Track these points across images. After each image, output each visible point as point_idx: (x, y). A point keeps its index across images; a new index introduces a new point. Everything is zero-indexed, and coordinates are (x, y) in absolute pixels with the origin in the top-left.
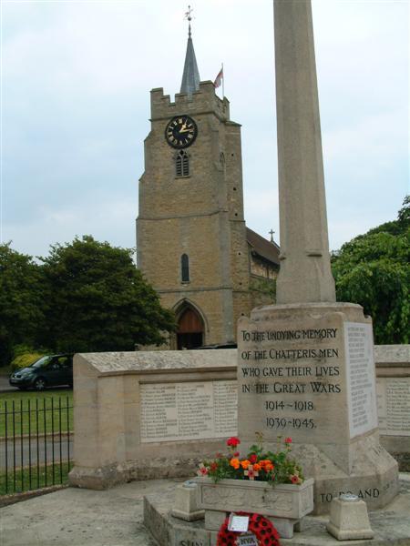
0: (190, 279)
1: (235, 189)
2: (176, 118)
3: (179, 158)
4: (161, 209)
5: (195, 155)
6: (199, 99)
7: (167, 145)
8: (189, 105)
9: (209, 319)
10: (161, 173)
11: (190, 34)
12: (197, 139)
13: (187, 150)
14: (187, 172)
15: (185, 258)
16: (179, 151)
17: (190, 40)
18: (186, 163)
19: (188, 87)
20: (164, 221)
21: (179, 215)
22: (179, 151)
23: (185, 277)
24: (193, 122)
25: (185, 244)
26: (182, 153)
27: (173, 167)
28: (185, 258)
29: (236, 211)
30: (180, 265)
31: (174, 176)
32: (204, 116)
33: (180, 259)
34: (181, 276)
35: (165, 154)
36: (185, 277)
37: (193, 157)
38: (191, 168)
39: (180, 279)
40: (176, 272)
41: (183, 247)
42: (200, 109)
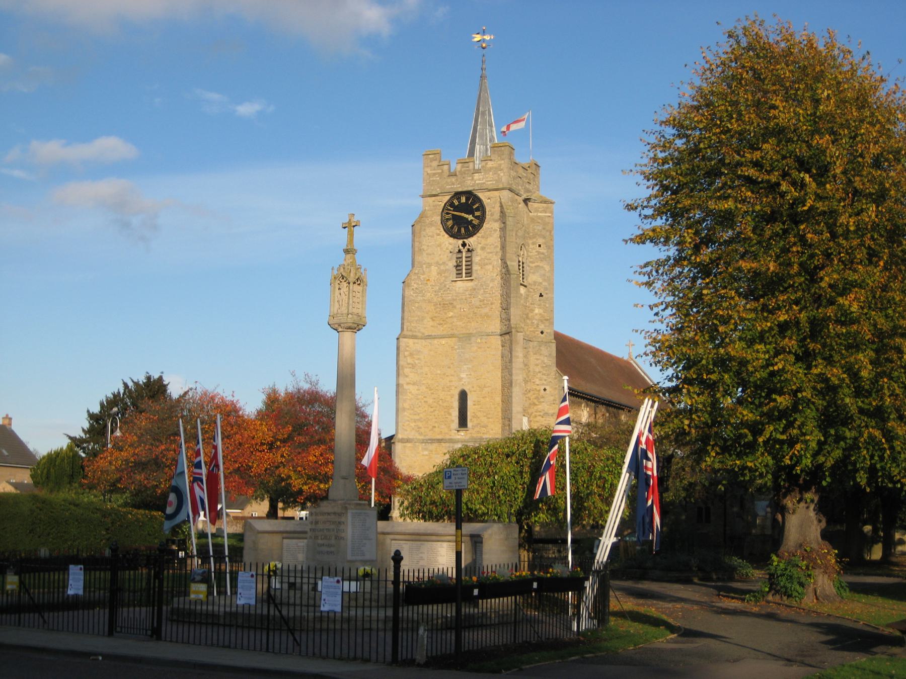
0: (469, 424)
1: (541, 295)
2: (458, 195)
3: (460, 251)
6: (491, 169)
8: (476, 176)
13: (471, 241)
14: (469, 273)
15: (463, 396)
16: (461, 242)
18: (469, 260)
19: (477, 147)
20: (436, 341)
23: (463, 422)
24: (480, 200)
25: (463, 375)
26: (464, 245)
28: (463, 396)
30: (456, 405)
31: (453, 276)
32: (496, 193)
33: (457, 397)
34: (457, 421)
35: (439, 245)
36: (463, 422)
37: (479, 251)
38: (475, 267)
40: (450, 414)
41: (461, 379)
42: (490, 184)
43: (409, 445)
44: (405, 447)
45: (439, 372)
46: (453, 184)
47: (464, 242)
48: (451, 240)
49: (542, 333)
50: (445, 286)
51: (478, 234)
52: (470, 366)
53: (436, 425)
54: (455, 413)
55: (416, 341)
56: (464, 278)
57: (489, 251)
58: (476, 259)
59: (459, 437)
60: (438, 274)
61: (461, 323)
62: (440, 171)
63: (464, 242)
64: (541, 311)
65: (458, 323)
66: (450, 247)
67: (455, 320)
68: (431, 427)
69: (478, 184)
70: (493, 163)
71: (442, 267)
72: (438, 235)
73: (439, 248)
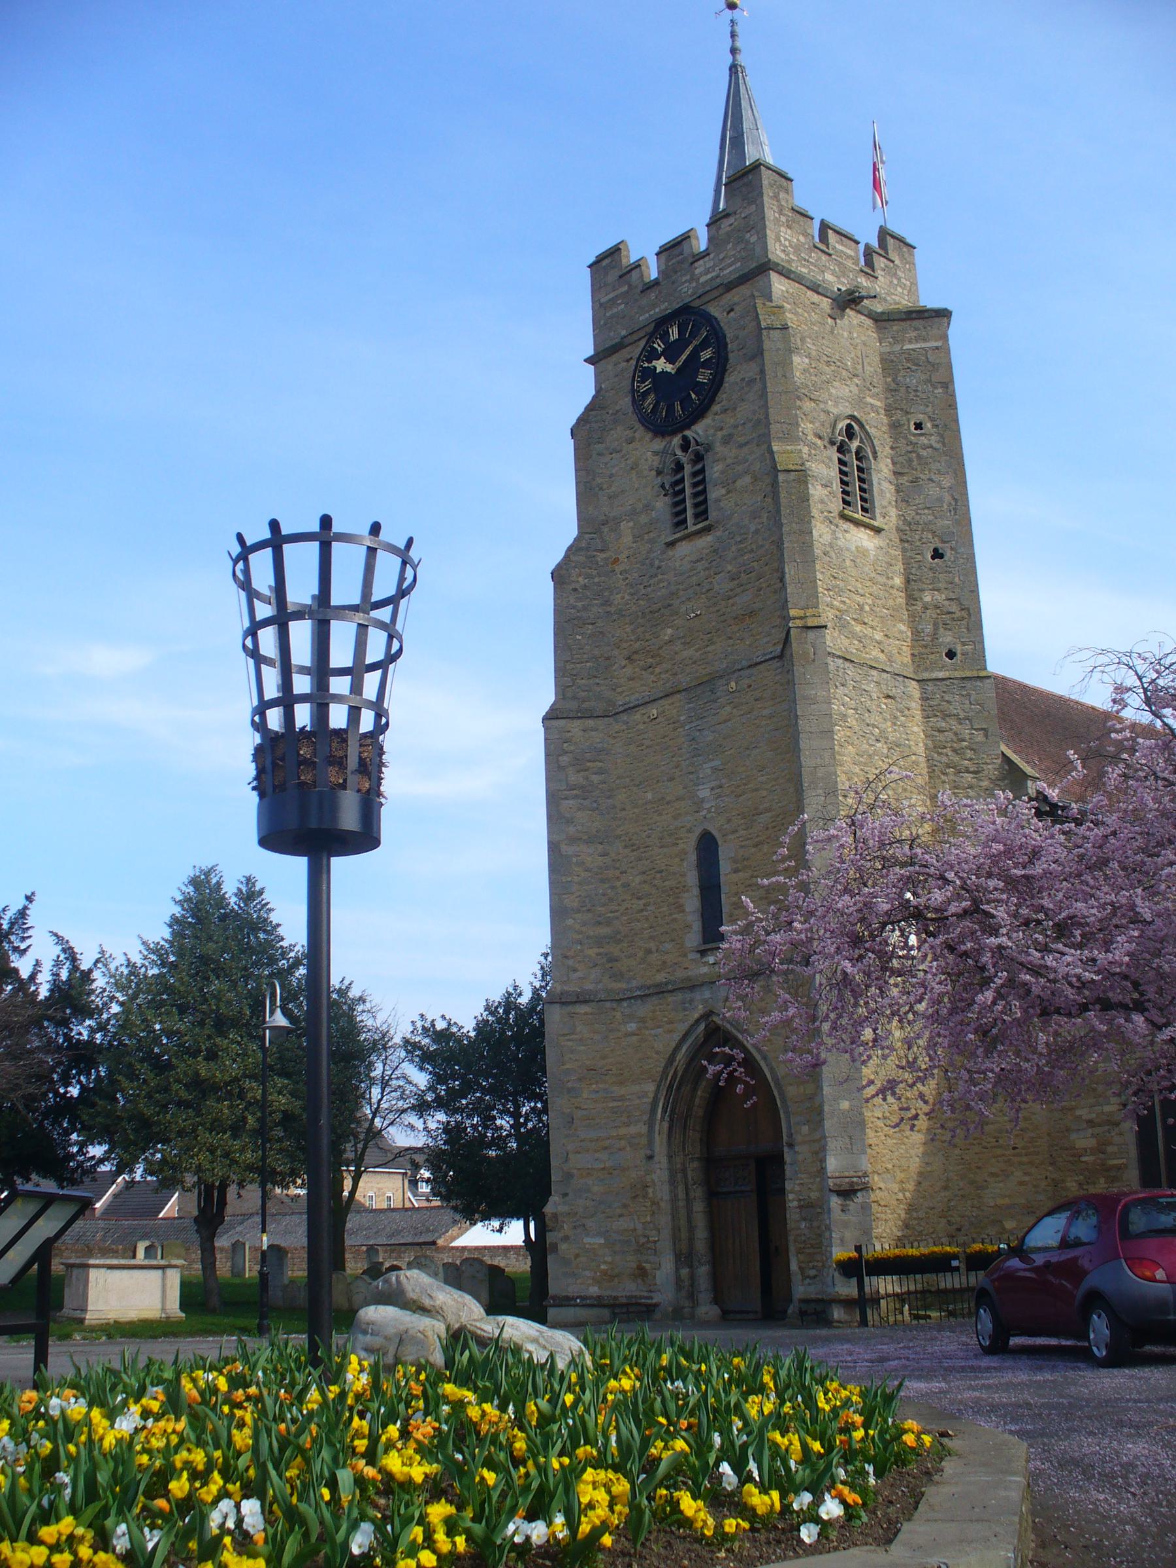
1: (937, 554)
4: (629, 671)
5: (727, 440)
7: (640, 431)
9: (791, 1091)
10: (627, 539)
11: (734, 51)
12: (731, 379)
13: (699, 431)
15: (707, 846)
16: (677, 440)
17: (734, 69)
21: (684, 680)
22: (677, 440)
24: (710, 320)
25: (704, 792)
26: (685, 446)
27: (662, 505)
28: (707, 846)
29: (947, 639)
33: (693, 857)
34: (697, 926)
37: (719, 448)
38: (714, 494)
39: (693, 938)
40: (681, 909)
41: (699, 804)
43: (583, 1009)
44: (571, 1015)
45: (649, 796)
46: (654, 306)
47: (685, 438)
48: (658, 444)
49: (951, 655)
50: (652, 565)
51: (716, 408)
52: (717, 763)
53: (652, 945)
54: (692, 902)
55: (590, 723)
56: (692, 528)
57: (741, 440)
58: (715, 471)
59: (705, 970)
60: (637, 538)
61: (690, 652)
62: (626, 288)
63: (685, 438)
64: (940, 597)
65: (685, 654)
66: (656, 462)
67: (678, 647)
68: (641, 954)
69: (704, 284)
70: (731, 220)
71: (644, 519)
72: (631, 441)
73: (634, 474)
